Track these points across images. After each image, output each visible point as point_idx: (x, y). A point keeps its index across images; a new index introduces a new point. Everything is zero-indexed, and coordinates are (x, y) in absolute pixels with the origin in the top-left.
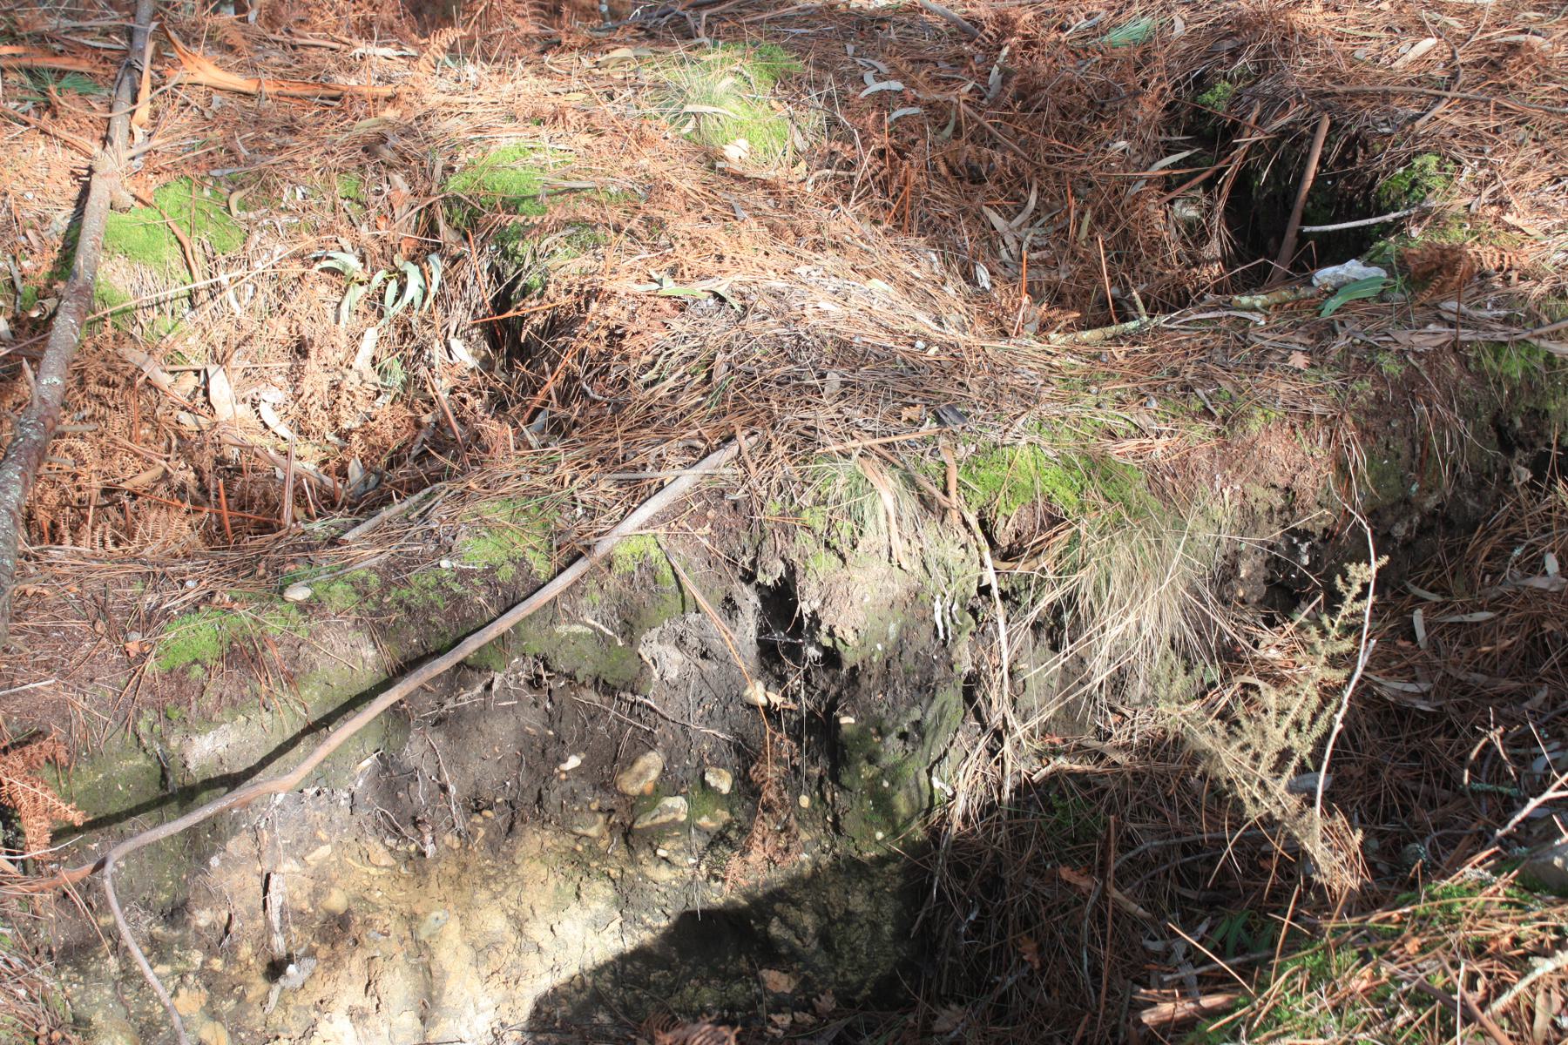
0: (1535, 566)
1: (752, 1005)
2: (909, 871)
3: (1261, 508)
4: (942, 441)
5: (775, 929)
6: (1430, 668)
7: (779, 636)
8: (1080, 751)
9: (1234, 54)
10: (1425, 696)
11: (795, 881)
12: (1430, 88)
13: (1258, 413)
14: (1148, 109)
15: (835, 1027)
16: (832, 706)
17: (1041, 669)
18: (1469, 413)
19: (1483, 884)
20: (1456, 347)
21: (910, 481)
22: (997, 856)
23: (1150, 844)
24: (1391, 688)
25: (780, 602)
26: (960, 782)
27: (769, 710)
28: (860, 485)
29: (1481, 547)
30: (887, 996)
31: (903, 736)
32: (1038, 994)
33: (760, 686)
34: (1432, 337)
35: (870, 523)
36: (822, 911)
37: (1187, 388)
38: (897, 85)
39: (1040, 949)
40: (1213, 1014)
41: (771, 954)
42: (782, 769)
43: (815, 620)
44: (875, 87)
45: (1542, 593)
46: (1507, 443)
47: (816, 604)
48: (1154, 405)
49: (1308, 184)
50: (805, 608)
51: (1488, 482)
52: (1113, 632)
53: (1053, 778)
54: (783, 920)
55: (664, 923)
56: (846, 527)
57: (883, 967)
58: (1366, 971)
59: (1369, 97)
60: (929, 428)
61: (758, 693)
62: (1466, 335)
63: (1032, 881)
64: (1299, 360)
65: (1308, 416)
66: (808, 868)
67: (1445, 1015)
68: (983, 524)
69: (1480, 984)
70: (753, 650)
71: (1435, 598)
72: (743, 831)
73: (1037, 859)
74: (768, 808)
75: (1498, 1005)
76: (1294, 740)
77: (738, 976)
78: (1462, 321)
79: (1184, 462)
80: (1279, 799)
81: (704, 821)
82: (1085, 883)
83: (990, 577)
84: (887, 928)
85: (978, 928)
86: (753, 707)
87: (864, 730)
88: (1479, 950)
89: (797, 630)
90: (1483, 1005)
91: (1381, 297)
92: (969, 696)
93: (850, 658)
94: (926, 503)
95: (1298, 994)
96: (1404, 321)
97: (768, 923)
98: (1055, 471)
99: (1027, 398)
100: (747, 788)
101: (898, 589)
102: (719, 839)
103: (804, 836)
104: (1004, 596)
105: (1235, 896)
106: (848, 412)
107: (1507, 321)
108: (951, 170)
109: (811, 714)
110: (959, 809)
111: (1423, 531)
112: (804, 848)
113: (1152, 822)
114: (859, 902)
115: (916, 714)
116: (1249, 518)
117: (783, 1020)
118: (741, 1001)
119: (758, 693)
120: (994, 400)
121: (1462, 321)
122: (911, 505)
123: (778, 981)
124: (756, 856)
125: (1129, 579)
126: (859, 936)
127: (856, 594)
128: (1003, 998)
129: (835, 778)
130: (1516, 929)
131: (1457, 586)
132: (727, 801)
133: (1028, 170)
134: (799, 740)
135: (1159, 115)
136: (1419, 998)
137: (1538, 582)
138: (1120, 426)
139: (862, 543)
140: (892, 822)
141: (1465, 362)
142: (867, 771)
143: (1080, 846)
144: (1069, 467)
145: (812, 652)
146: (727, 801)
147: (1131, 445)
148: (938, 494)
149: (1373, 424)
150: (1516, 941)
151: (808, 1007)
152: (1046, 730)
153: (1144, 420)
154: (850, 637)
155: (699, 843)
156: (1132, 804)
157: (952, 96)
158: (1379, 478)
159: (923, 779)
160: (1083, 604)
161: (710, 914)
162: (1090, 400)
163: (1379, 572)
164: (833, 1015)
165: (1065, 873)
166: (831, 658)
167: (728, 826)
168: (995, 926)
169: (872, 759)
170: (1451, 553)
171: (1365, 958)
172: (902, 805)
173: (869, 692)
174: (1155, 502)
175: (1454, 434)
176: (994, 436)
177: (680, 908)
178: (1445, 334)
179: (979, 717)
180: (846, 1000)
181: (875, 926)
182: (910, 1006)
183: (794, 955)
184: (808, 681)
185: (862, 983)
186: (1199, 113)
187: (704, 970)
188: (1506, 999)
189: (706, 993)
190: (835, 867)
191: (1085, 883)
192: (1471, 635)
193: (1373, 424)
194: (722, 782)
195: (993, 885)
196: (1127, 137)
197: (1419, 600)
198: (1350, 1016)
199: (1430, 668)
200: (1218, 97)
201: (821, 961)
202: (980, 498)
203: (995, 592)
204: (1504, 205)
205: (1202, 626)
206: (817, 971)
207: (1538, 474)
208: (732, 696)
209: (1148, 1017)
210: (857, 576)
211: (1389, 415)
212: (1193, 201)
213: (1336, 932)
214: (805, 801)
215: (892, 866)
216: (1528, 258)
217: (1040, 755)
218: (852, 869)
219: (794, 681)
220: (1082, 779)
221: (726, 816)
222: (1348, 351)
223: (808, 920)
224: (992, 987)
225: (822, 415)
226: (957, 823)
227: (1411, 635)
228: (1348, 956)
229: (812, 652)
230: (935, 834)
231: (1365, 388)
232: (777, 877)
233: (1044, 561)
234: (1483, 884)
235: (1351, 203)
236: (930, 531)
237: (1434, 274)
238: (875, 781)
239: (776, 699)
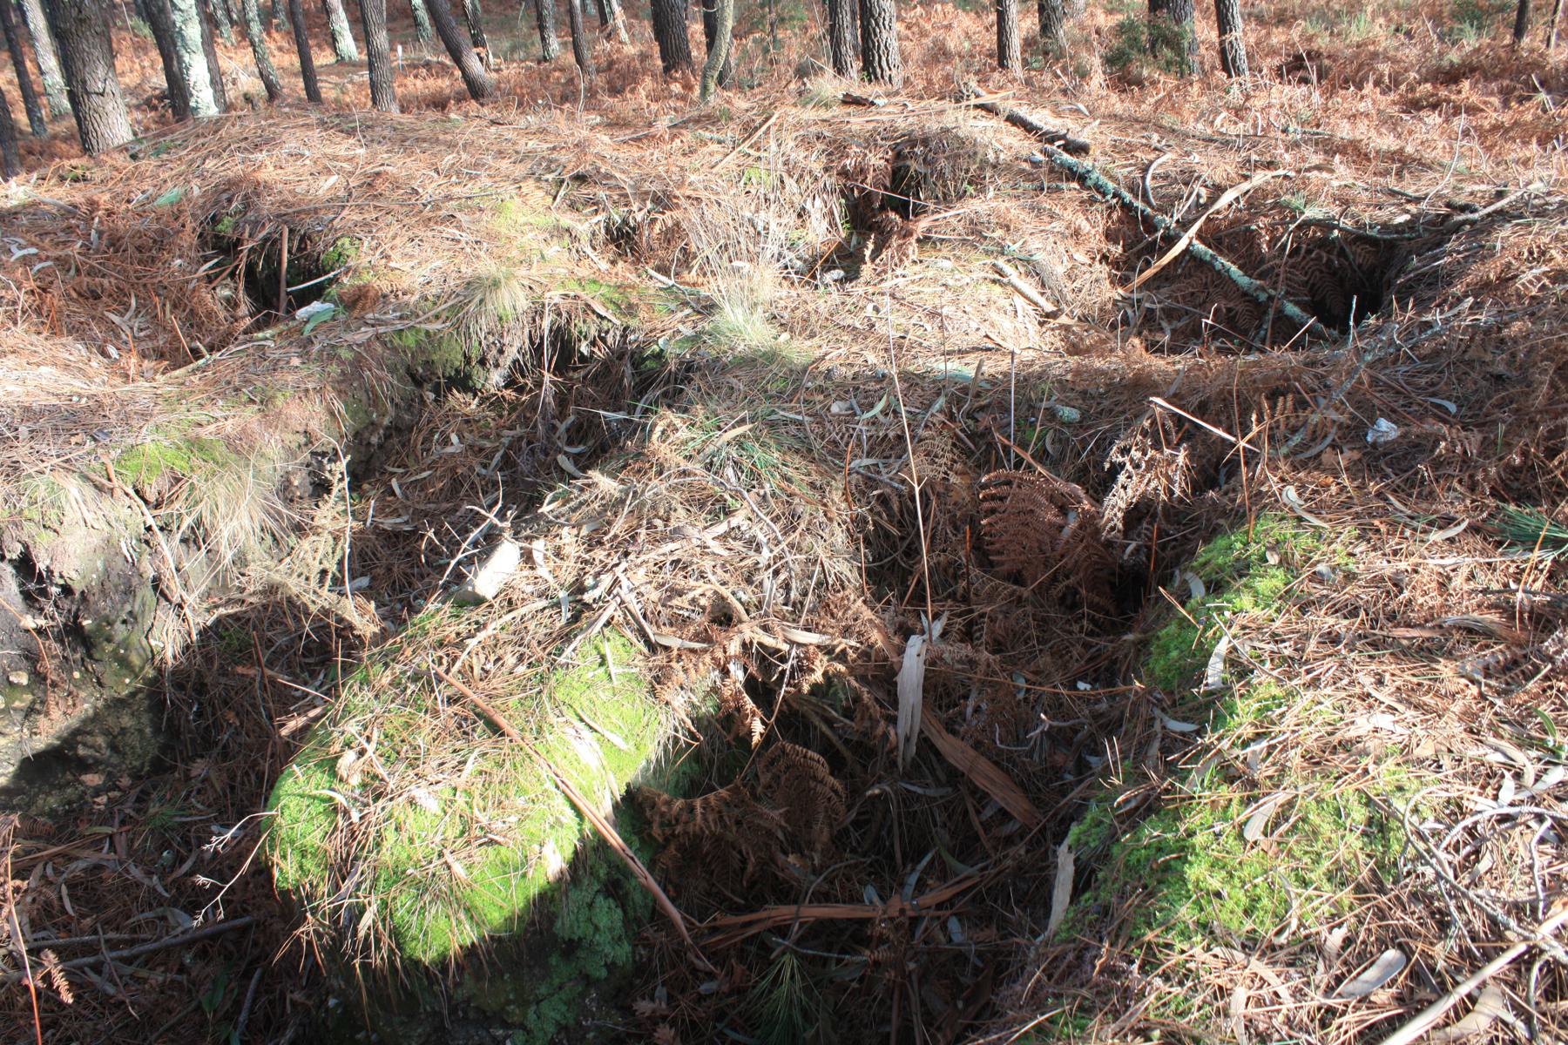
0: (446, 441)
1: (81, 797)
2: (150, 695)
3: (294, 446)
4: (100, 451)
5: (81, 751)
6: (406, 508)
7: (32, 586)
8: (229, 602)
9: (230, 201)
10: (406, 523)
11: (85, 722)
12: (337, 204)
13: (279, 395)
14: (188, 239)
15: (134, 793)
16: (76, 617)
17: (195, 561)
18: (393, 370)
19: (438, 611)
21: (86, 478)
22: (198, 672)
23: (281, 641)
24: (388, 523)
25: (25, 565)
26: (167, 638)
27: (40, 631)
28: (53, 488)
29: (417, 438)
30: (158, 767)
31: (124, 622)
32: (243, 739)
33: (29, 617)
34: (364, 334)
35: (67, 508)
36: (107, 733)
37: (237, 390)
38: (33, 250)
39: (237, 714)
40: (317, 719)
41: (84, 766)
42: (56, 661)
43: (50, 571)
44: (19, 254)
45: (452, 455)
46: (418, 382)
47: (48, 562)
48: (220, 403)
49: (285, 265)
50: (41, 566)
51: (413, 404)
52: (226, 534)
53: (219, 621)
54: (85, 745)
55: (12, 769)
56: (52, 514)
57: (153, 751)
58: (388, 672)
59: (307, 212)
60: (90, 445)
61: (29, 622)
62: (381, 330)
63: (223, 680)
64: (296, 362)
65: (307, 390)
66: (91, 712)
67: (429, 683)
68: (137, 492)
69: (444, 661)
70: (19, 598)
71: (401, 470)
72: (43, 702)
73: (222, 667)
74: (54, 685)
75: (454, 669)
76: (326, 565)
77: (68, 784)
79: (244, 430)
80: (327, 597)
81: (17, 704)
82: (252, 672)
83: (150, 521)
84: (148, 730)
85: (199, 714)
86: (27, 631)
87: (99, 625)
88: (441, 644)
89: (41, 579)
90: (447, 671)
91: (333, 319)
92: (155, 588)
93: (78, 587)
94: (99, 488)
95: (355, 695)
96: (348, 329)
97: (76, 749)
98: (171, 453)
99: (145, 415)
100: (38, 678)
101: (96, 540)
102: (30, 712)
103: (83, 694)
104: (162, 529)
105: (320, 654)
106: (37, 447)
107: (401, 318)
108: (80, 294)
109: (65, 625)
110: (169, 654)
111: (388, 437)
112: (85, 701)
113: (279, 629)
114: (127, 721)
115: (128, 608)
116: (291, 454)
117: (103, 799)
118: (74, 797)
119: (29, 622)
120: (126, 420)
122: (90, 491)
123: (93, 779)
124: (56, 714)
125: (228, 501)
126: (133, 739)
127: (71, 550)
128: (224, 747)
129: (90, 657)
130: (457, 629)
131: (410, 462)
132: (28, 688)
133: (126, 287)
134: (62, 642)
135: (196, 241)
136: (416, 678)
137: (449, 449)
138: (203, 419)
139: (65, 520)
140: (133, 671)
142: (109, 648)
143: (244, 653)
144: (179, 448)
145: (54, 590)
146: (28, 688)
147: (212, 428)
148: (105, 481)
149: (343, 387)
150: (458, 634)
151: (116, 787)
152: (208, 594)
153: (218, 414)
154: (74, 575)
155: (18, 717)
156: (266, 623)
157: (69, 251)
159: (144, 642)
160: (207, 521)
161: (39, 756)
162: (183, 408)
163: (348, 465)
164: (131, 787)
165: (240, 670)
166: (67, 590)
167: (34, 702)
168: (209, 710)
169: (109, 640)
170: (403, 446)
171: (386, 665)
172: (136, 660)
173: (96, 603)
174: (234, 456)
175: (388, 383)
176: (130, 441)
177: (19, 757)
179: (167, 599)
180: (136, 776)
181: (141, 731)
182: (173, 768)
183: (97, 762)
184: (57, 607)
185: (143, 765)
187: (46, 788)
188: (458, 664)
189: (51, 800)
190: (107, 707)
191: (252, 672)
192: (422, 485)
193: (343, 387)
194: (22, 678)
195: (201, 688)
196: (180, 257)
197: (393, 474)
198: (383, 697)
199: (406, 508)
200: (226, 226)
201: (115, 760)
202: (131, 477)
203: (155, 529)
204: (388, 257)
205: (277, 516)
206: (114, 766)
207: (438, 394)
208: (15, 628)
209: (284, 732)
210: (68, 539)
211: (350, 380)
212: (226, 286)
213: (370, 657)
214: (77, 675)
215: (140, 695)
217: (208, 610)
218: (118, 704)
219: (49, 609)
220: (235, 617)
221: (30, 697)
222: (321, 351)
223: (101, 740)
224: (217, 744)
225: (21, 452)
226: (170, 661)
227: (393, 493)
228: (379, 667)
229: (54, 590)
230: (160, 670)
231: (334, 369)
232: (73, 722)
233: (177, 505)
234: (438, 611)
235: (310, 271)
236: (106, 503)
237: (357, 301)
238: (115, 652)
239: (41, 622)
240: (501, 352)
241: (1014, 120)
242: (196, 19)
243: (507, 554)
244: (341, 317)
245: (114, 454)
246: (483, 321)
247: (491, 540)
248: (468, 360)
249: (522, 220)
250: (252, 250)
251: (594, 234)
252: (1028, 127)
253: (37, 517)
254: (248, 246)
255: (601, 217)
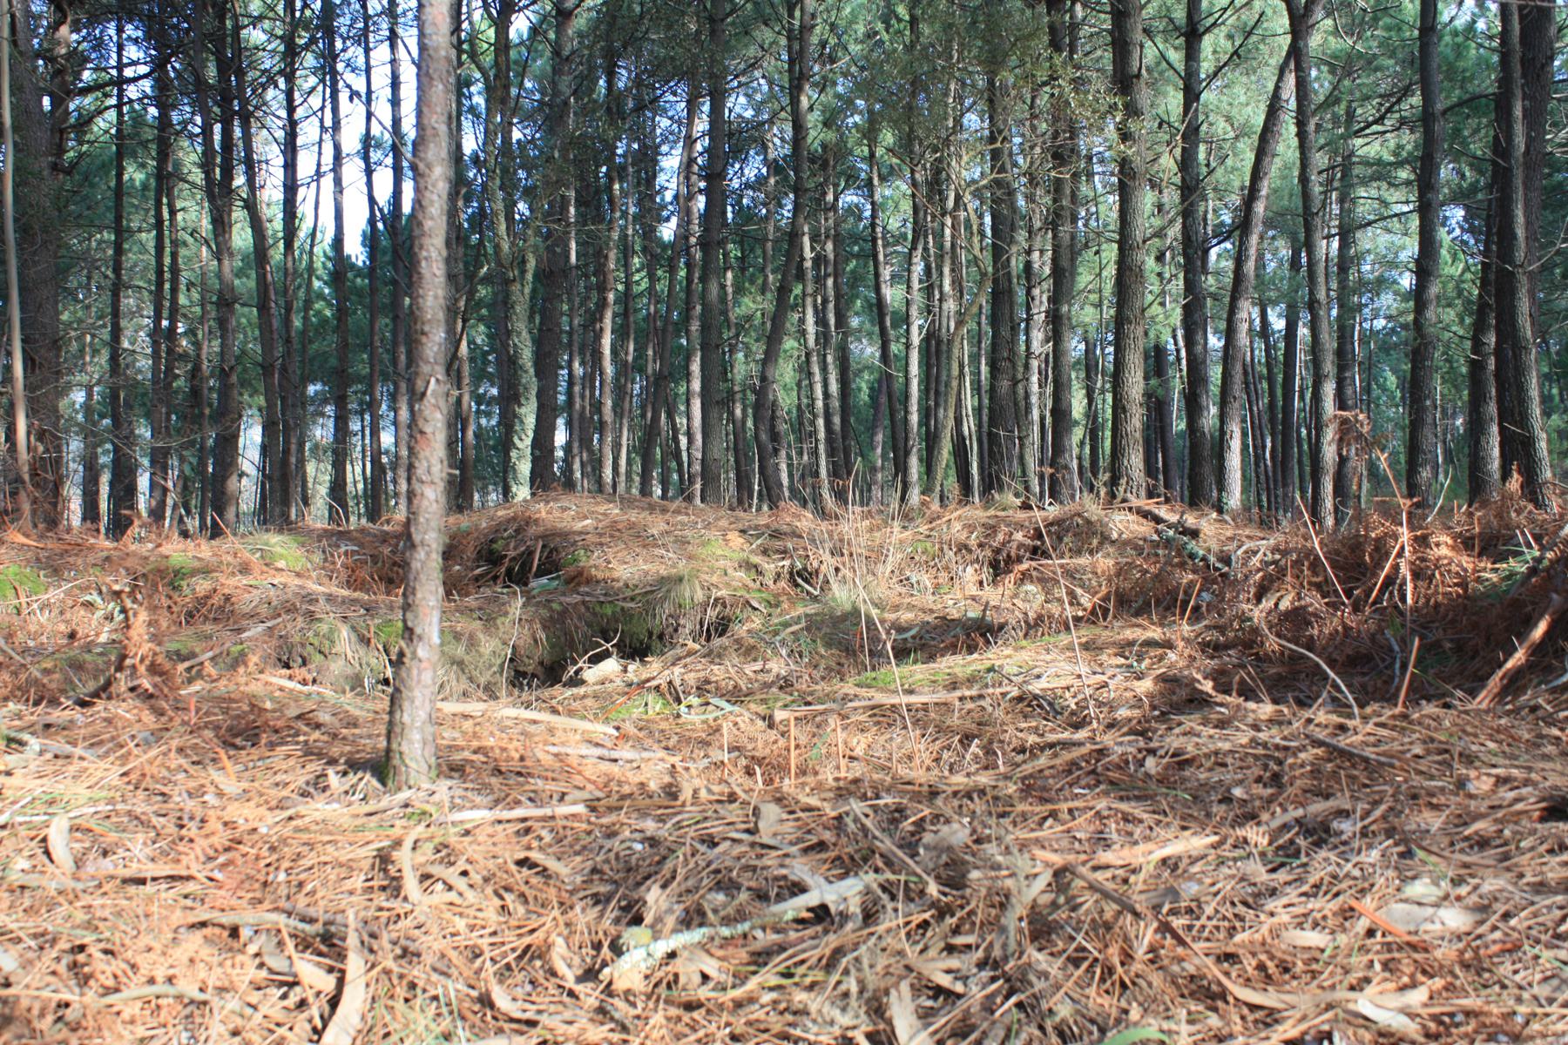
18: (589, 625)
20: (583, 602)
21: (354, 628)
34: (577, 598)
59: (560, 535)
78: (588, 594)
96: (564, 594)
101: (349, 671)
121: (588, 594)
122: (354, 638)
141: (588, 608)
158: (553, 646)
178: (579, 598)
186: (491, 552)
200: (498, 546)
216: (616, 575)
231: (544, 613)
240: (676, 630)
241: (1145, 514)
242: (529, 458)
243: (611, 666)
244: (561, 588)
245: (377, 621)
246: (666, 605)
247: (605, 655)
248: (650, 634)
249: (719, 552)
250: (513, 559)
251: (778, 575)
252: (1158, 520)
253: (316, 643)
254: (512, 554)
255: (787, 563)
